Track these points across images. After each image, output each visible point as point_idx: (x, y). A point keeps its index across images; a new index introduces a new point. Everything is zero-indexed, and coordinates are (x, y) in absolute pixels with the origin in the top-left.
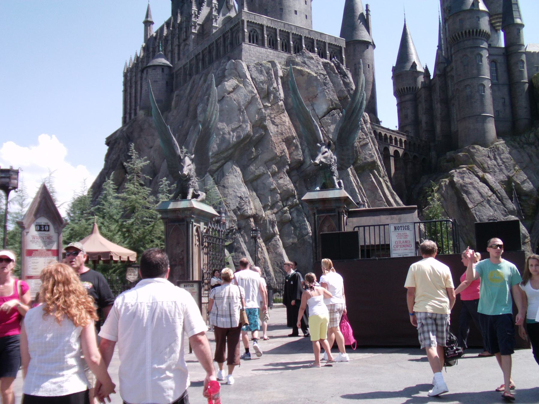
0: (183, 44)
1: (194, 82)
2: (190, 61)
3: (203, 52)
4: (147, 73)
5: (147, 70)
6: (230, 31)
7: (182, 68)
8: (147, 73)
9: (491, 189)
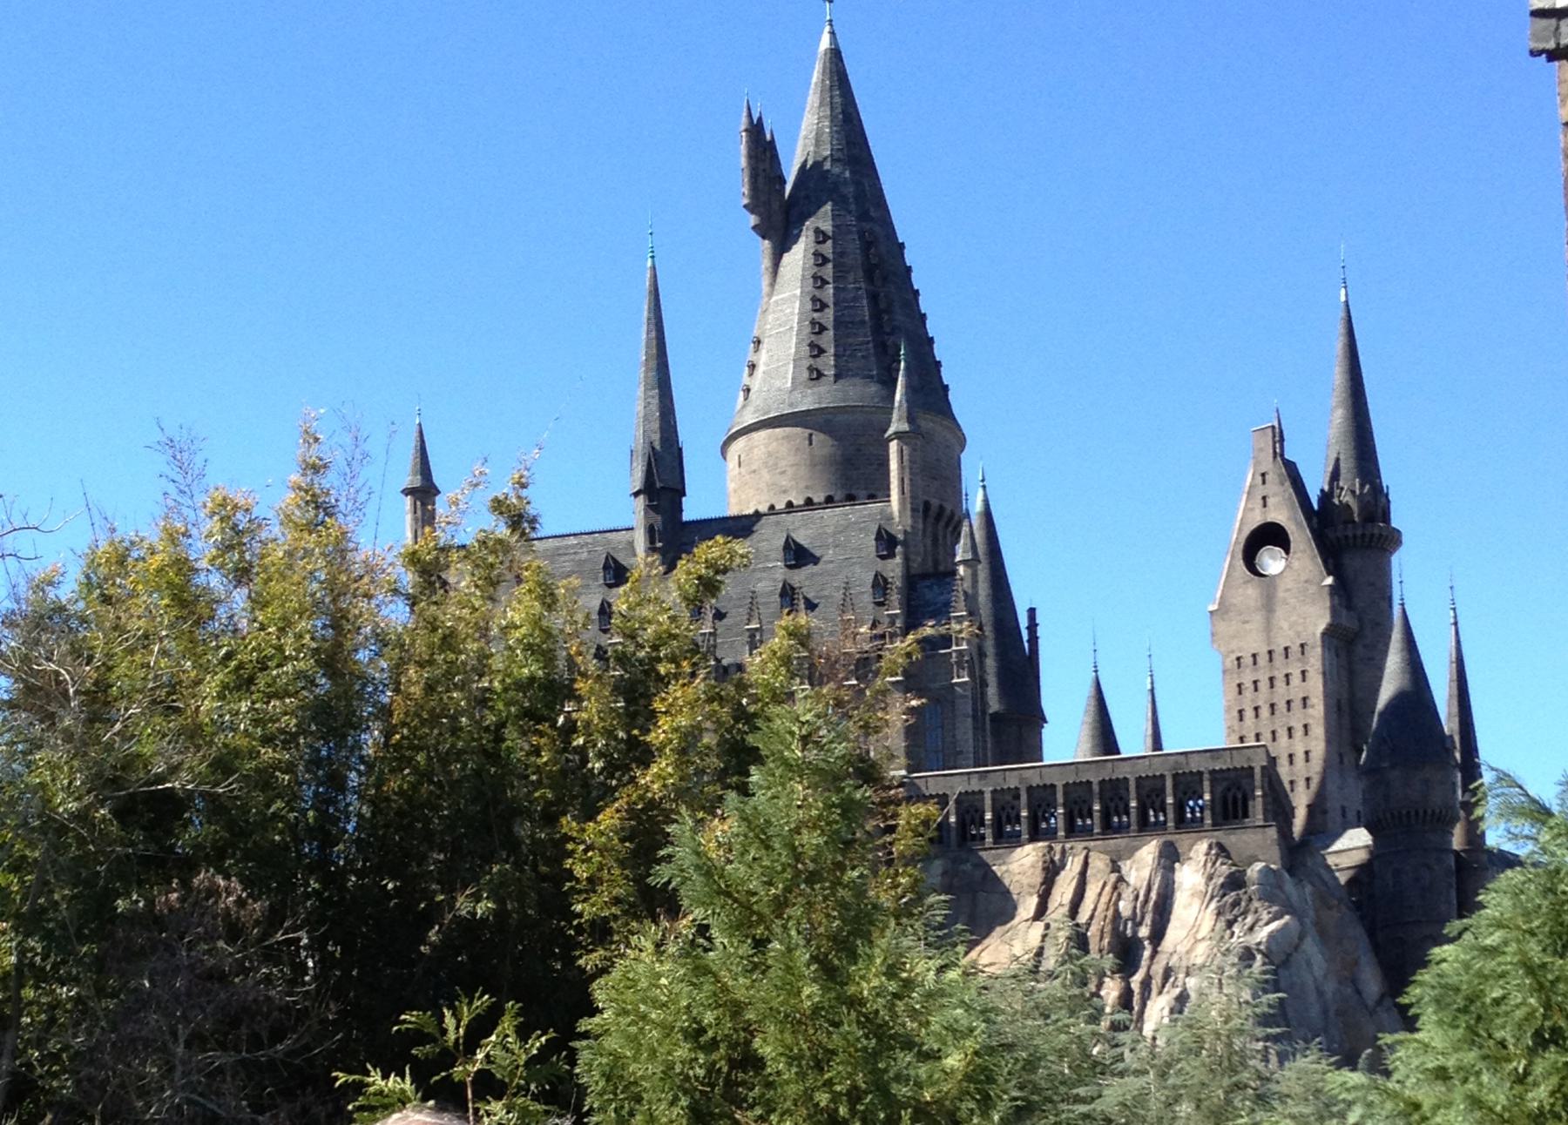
3: (1066, 786)
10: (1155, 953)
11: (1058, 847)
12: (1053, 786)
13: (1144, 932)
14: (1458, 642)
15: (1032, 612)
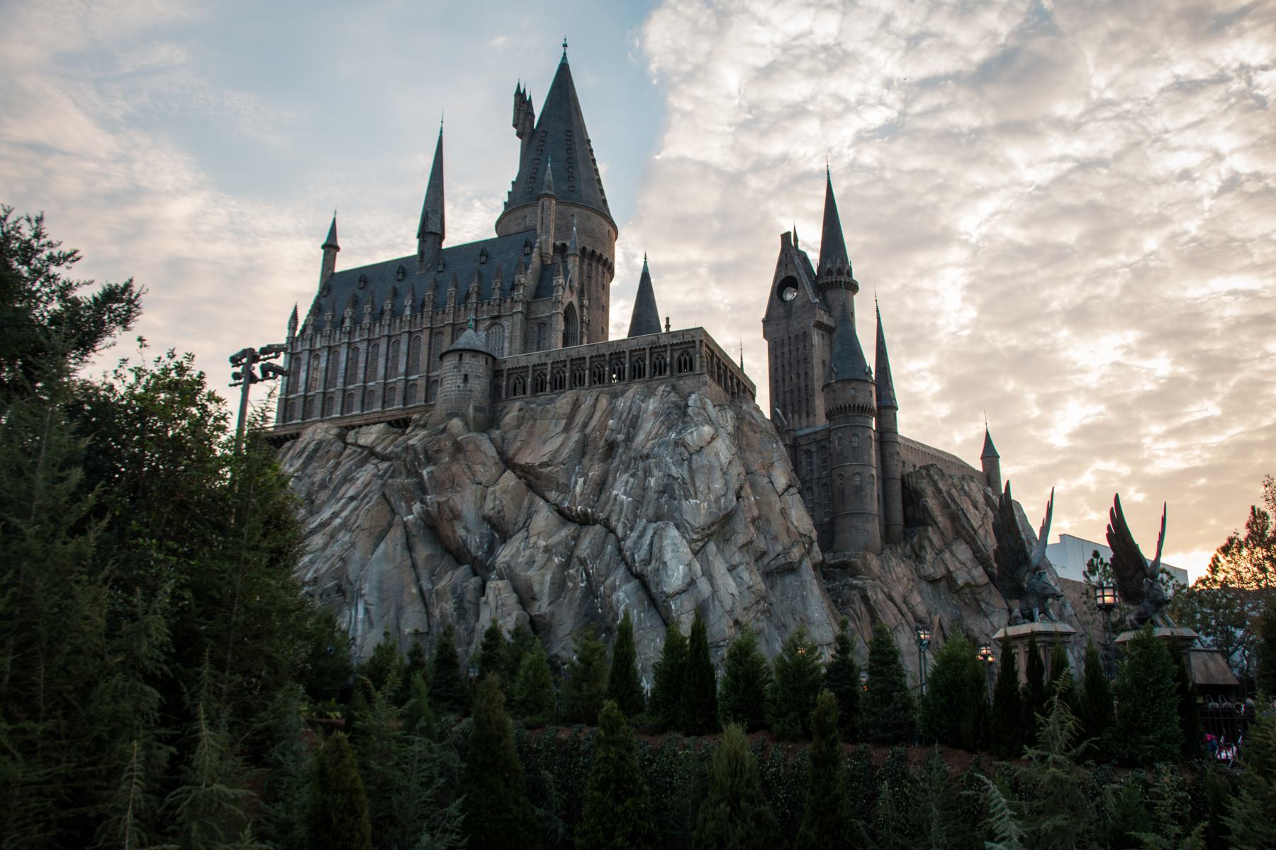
0: (488, 323)
1: (577, 399)
2: (553, 363)
3: (591, 357)
4: (461, 359)
5: (461, 355)
6: (669, 348)
7: (531, 369)
8: (461, 359)
9: (900, 611)
10: (627, 448)
11: (583, 392)
12: (584, 358)
13: (621, 437)
14: (879, 318)
15: (668, 319)
